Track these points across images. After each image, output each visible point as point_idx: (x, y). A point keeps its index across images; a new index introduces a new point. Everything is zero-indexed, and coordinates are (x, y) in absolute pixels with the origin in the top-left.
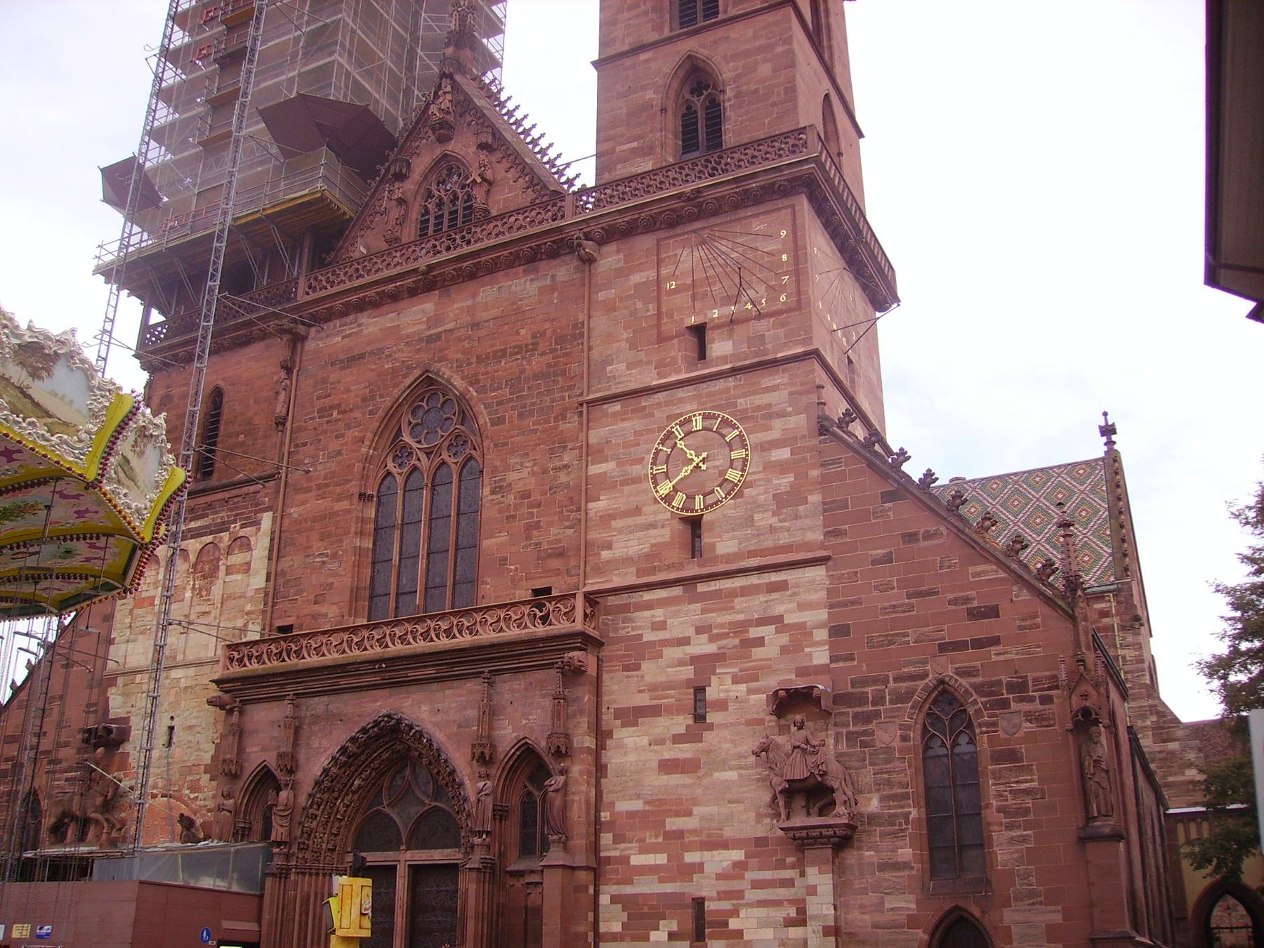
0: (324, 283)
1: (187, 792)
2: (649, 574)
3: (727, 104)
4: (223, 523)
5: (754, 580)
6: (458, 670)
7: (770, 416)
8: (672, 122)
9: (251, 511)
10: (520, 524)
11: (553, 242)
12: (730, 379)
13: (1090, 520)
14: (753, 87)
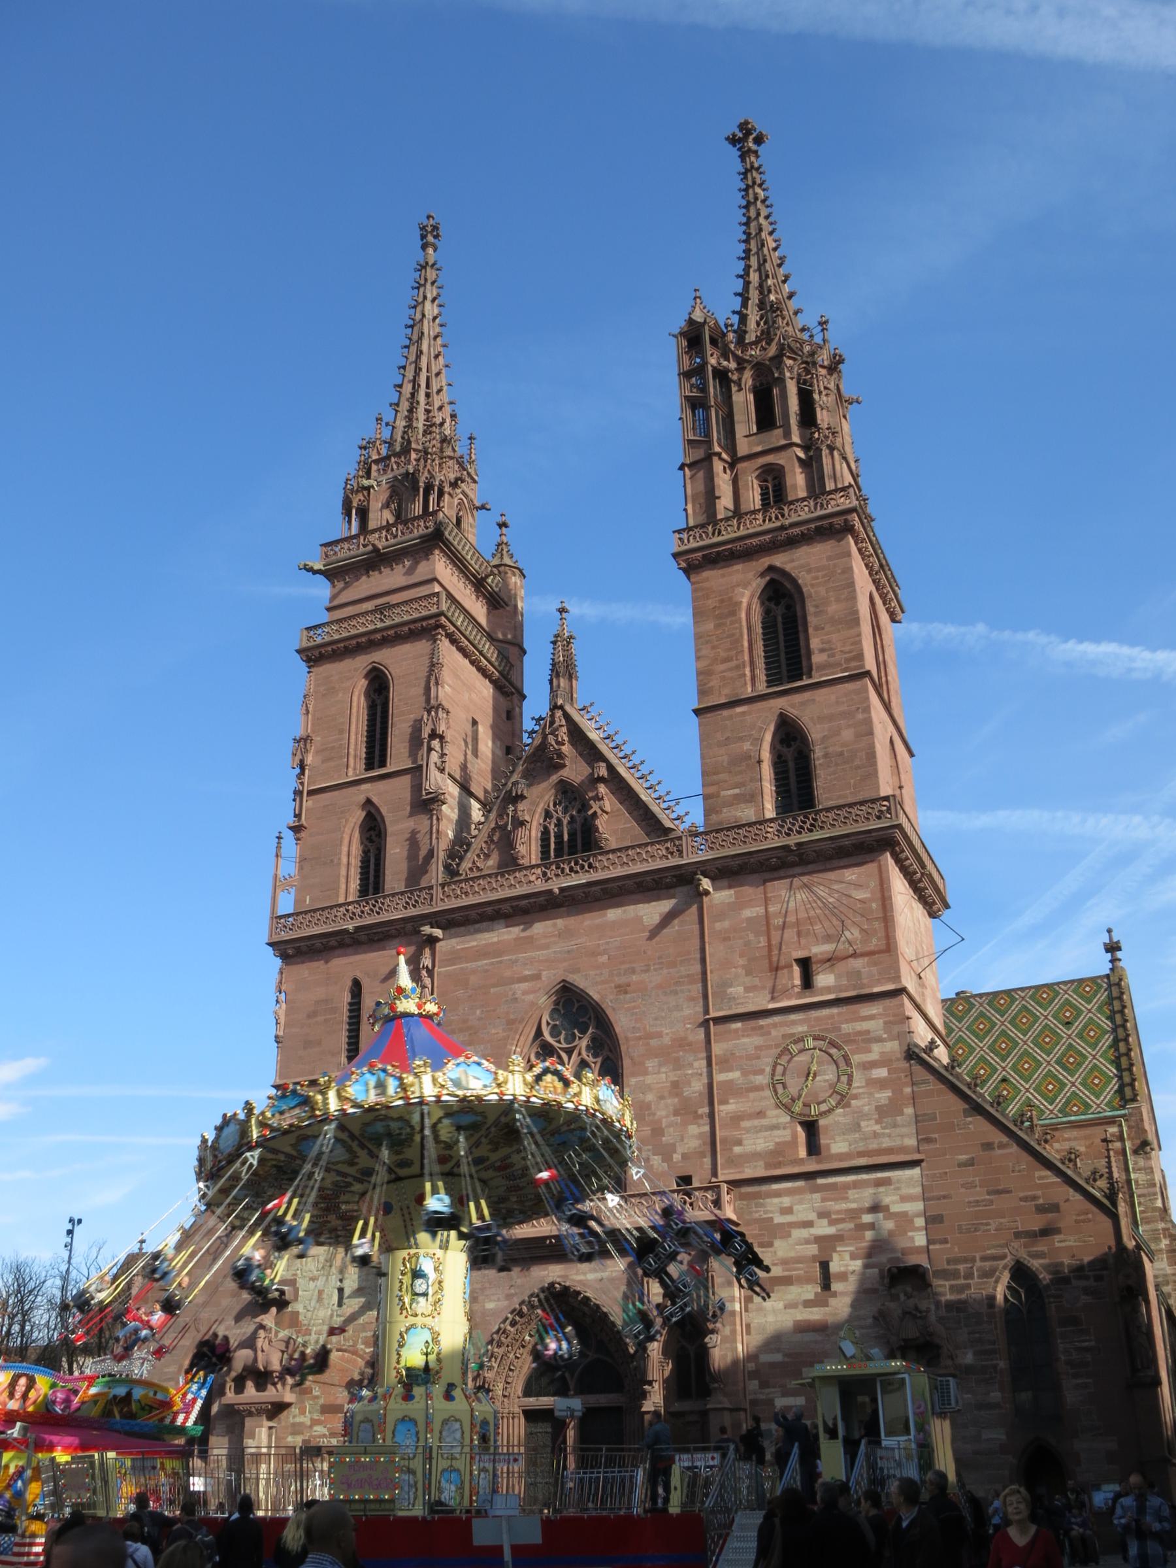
1: (363, 1347)
2: (775, 1168)
3: (817, 763)
11: (674, 876)
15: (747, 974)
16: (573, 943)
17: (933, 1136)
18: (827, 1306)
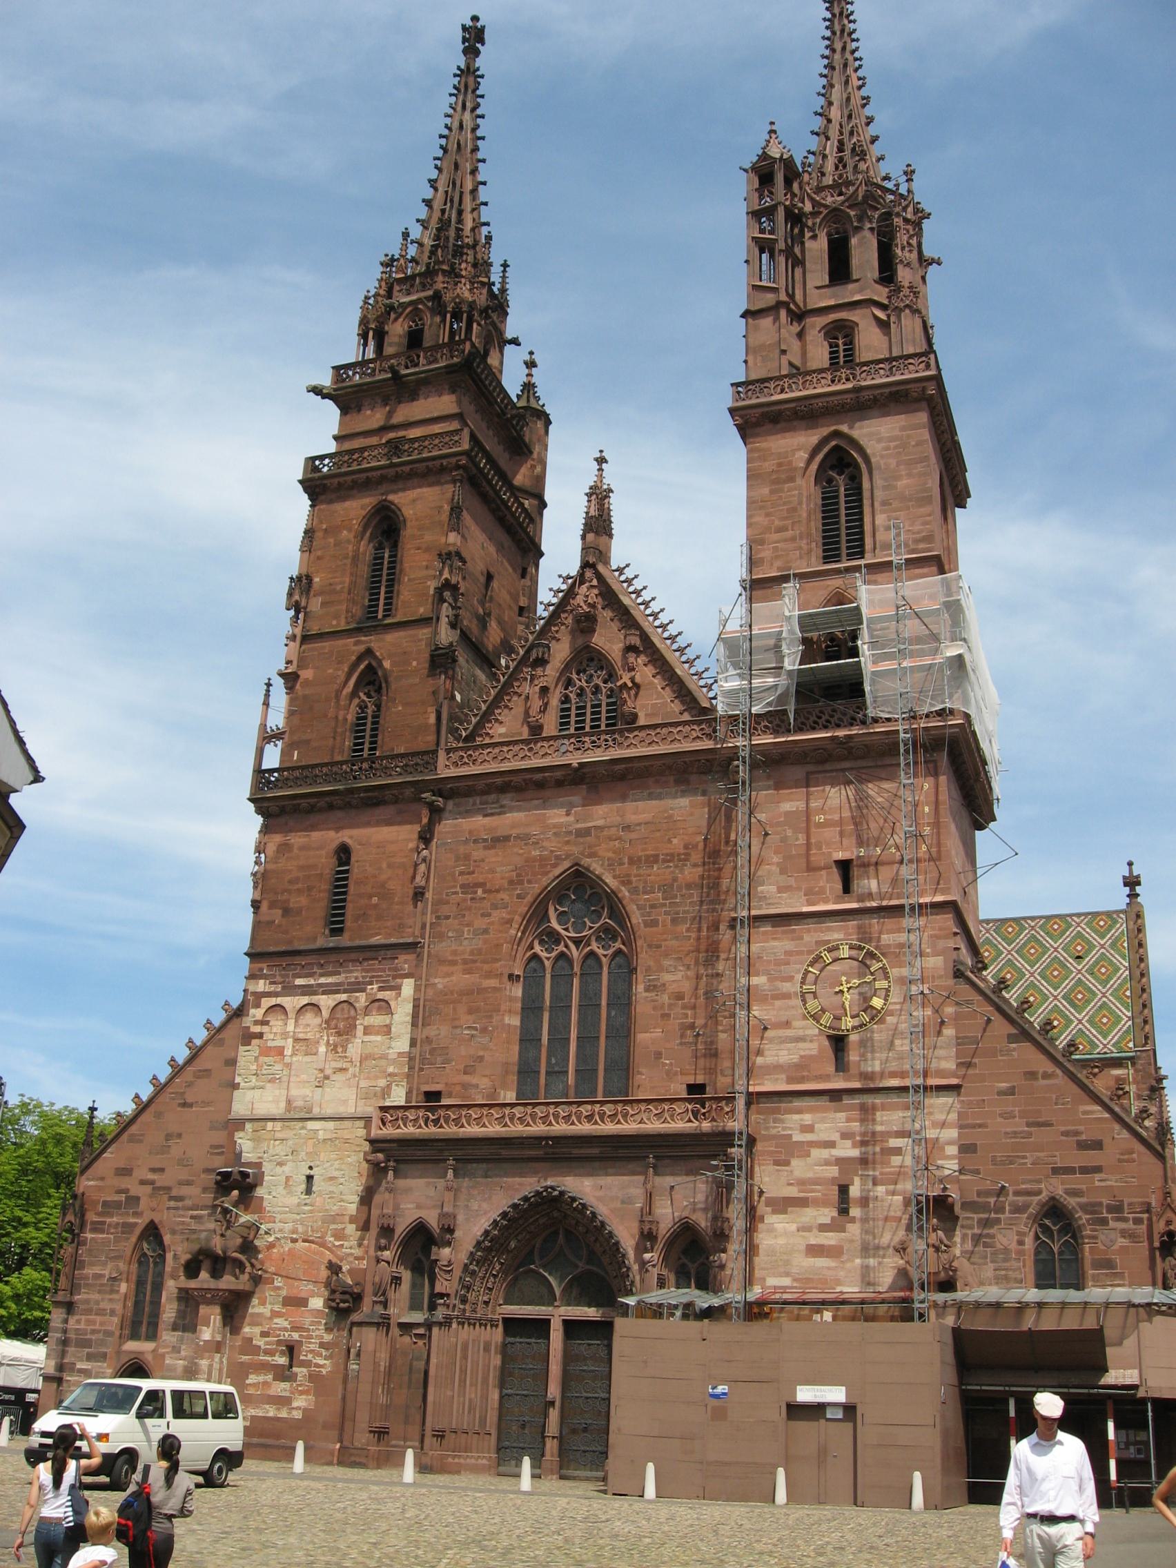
2: (799, 1082)
4: (358, 983)
6: (622, 1152)
10: (675, 1024)
13: (1109, 978)
15: (781, 873)
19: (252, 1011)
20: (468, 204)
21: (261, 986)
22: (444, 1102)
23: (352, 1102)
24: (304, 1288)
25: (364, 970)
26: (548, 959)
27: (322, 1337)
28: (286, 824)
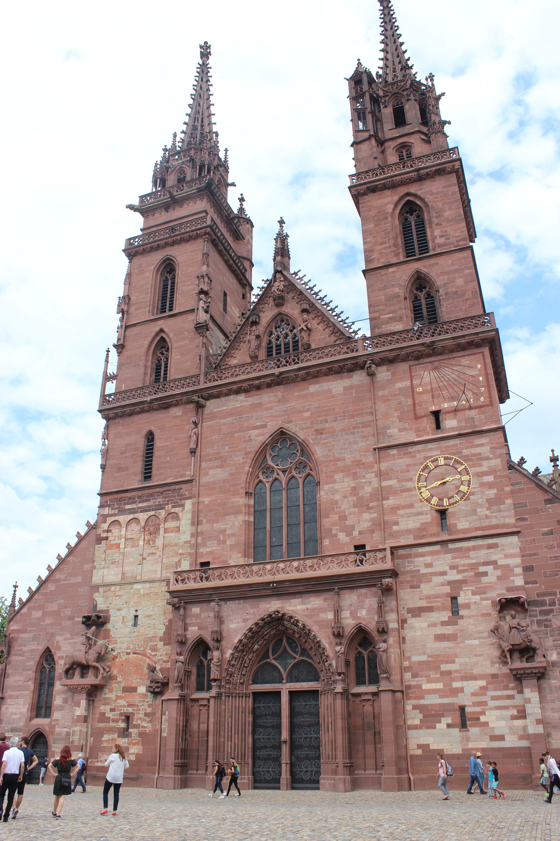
0: (216, 378)
1: (150, 651)
2: (421, 539)
3: (441, 298)
4: (160, 505)
5: (479, 542)
7: (481, 459)
8: (408, 304)
9: (178, 499)
11: (352, 364)
12: (457, 439)
14: (454, 290)
15: (400, 421)
16: (288, 406)
17: (525, 516)
18: (457, 625)
19: (103, 525)
20: (206, 122)
21: (106, 511)
22: (211, 566)
23: (159, 572)
24: (134, 681)
25: (163, 497)
26: (268, 482)
27: (146, 710)
28: (119, 422)
